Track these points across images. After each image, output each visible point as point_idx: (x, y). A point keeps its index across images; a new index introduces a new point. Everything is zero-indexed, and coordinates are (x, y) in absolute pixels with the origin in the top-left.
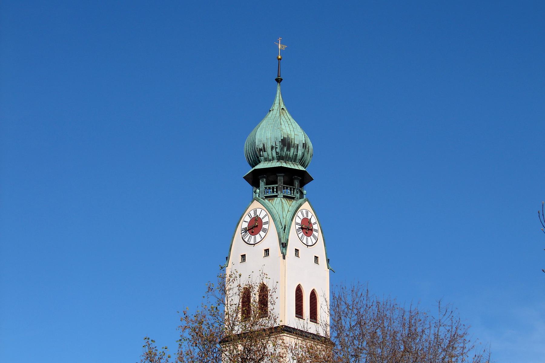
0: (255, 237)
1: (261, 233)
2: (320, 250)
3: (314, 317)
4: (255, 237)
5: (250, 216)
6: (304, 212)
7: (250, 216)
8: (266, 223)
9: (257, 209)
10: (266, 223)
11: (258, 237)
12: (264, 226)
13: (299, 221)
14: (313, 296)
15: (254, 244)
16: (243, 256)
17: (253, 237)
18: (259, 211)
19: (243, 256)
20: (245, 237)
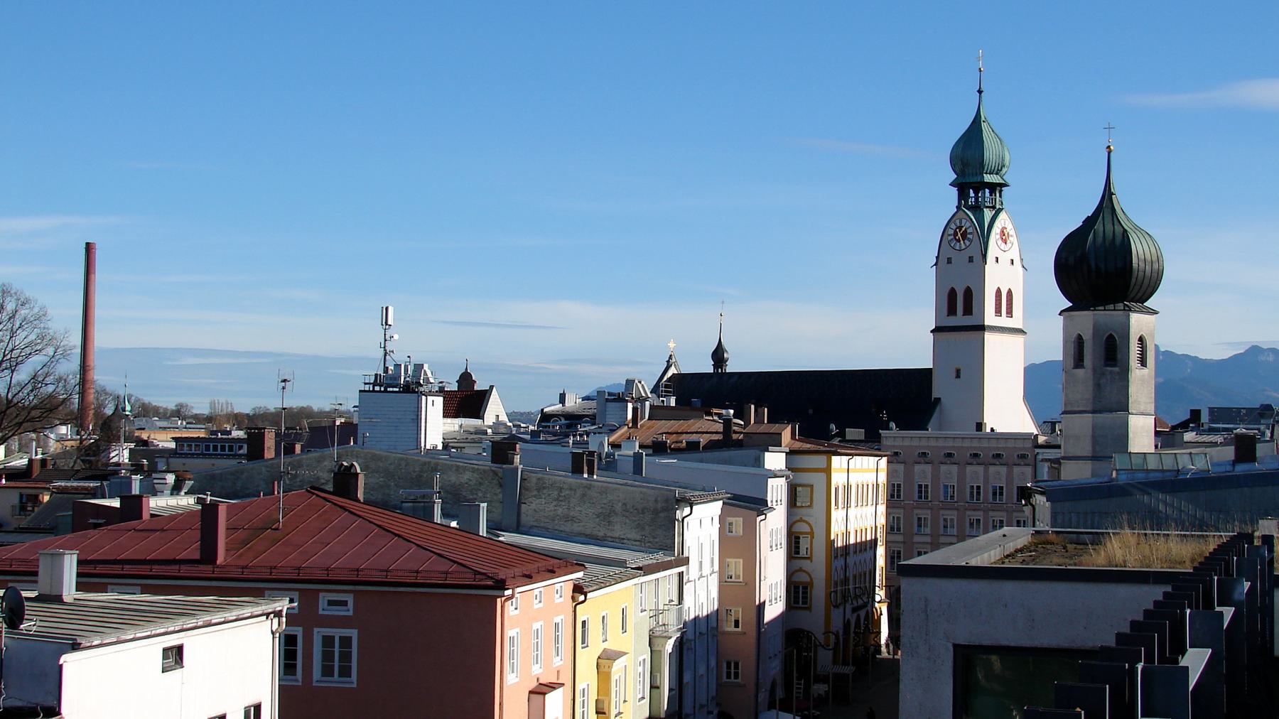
2: (1014, 253)
3: (1010, 313)
6: (1003, 221)
8: (970, 233)
10: (970, 233)
13: (999, 231)
14: (1010, 293)
16: (949, 261)
18: (964, 221)
19: (949, 261)
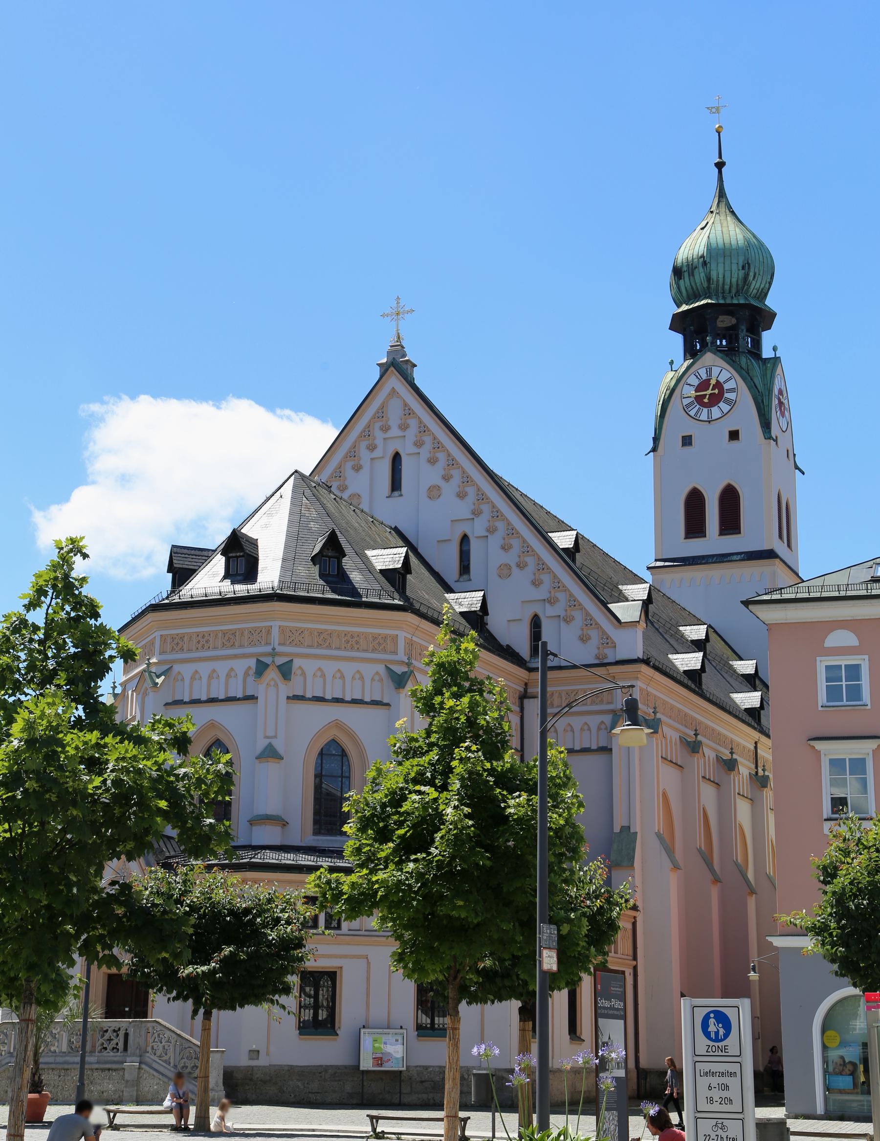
0: (710, 411)
1: (721, 404)
4: (710, 411)
5: (699, 376)
7: (699, 376)
9: (713, 367)
11: (716, 412)
12: (726, 395)
15: (709, 422)
16: (687, 441)
17: (705, 410)
18: (715, 371)
19: (687, 441)
20: (689, 409)
